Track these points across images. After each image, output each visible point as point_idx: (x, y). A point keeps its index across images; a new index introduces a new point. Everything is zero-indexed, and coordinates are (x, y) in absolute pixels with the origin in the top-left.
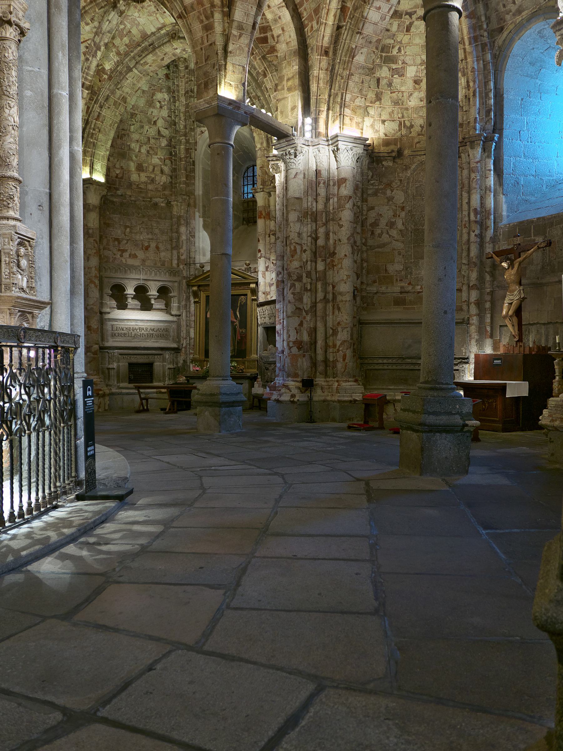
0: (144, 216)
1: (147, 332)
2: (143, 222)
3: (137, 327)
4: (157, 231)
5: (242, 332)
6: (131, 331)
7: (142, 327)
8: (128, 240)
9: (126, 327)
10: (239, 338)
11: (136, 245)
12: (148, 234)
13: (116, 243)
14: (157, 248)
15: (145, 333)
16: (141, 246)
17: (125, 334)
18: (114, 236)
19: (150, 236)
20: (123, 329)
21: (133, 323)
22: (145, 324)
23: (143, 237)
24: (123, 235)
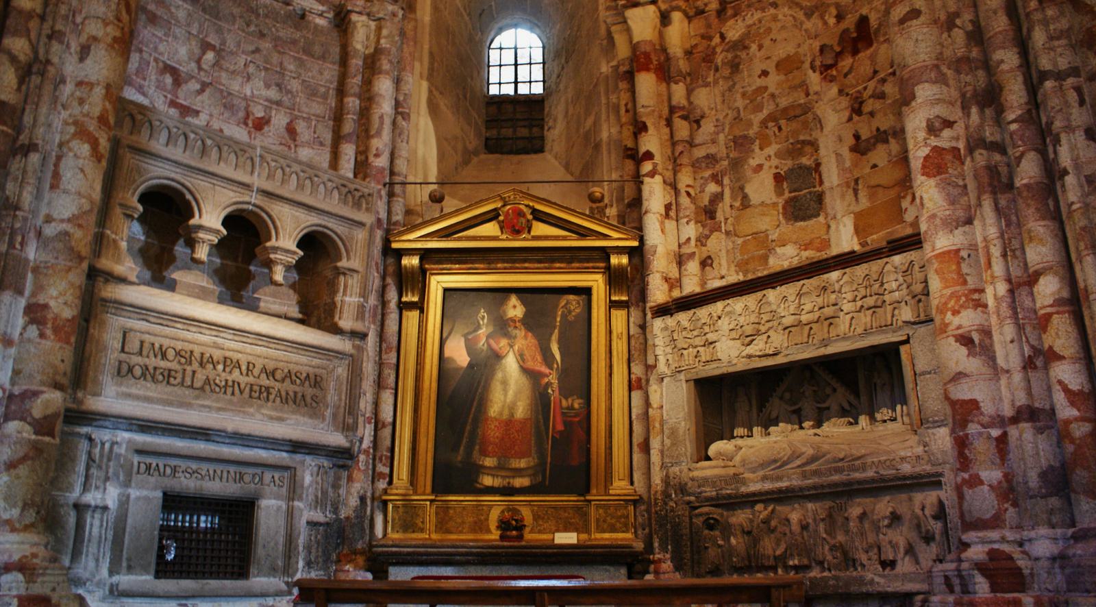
0: (262, 35)
1: (251, 379)
2: (257, 50)
3: (217, 354)
4: (295, 85)
5: (571, 408)
6: (195, 365)
7: (235, 356)
8: (204, 86)
9: (179, 346)
10: (560, 427)
11: (229, 107)
12: (268, 86)
13: (168, 80)
14: (291, 130)
15: (243, 380)
16: (241, 114)
17: (168, 375)
18: (165, 58)
19: (273, 93)
20: (164, 356)
21: (206, 338)
22: (249, 348)
23: (257, 89)
24: (193, 65)
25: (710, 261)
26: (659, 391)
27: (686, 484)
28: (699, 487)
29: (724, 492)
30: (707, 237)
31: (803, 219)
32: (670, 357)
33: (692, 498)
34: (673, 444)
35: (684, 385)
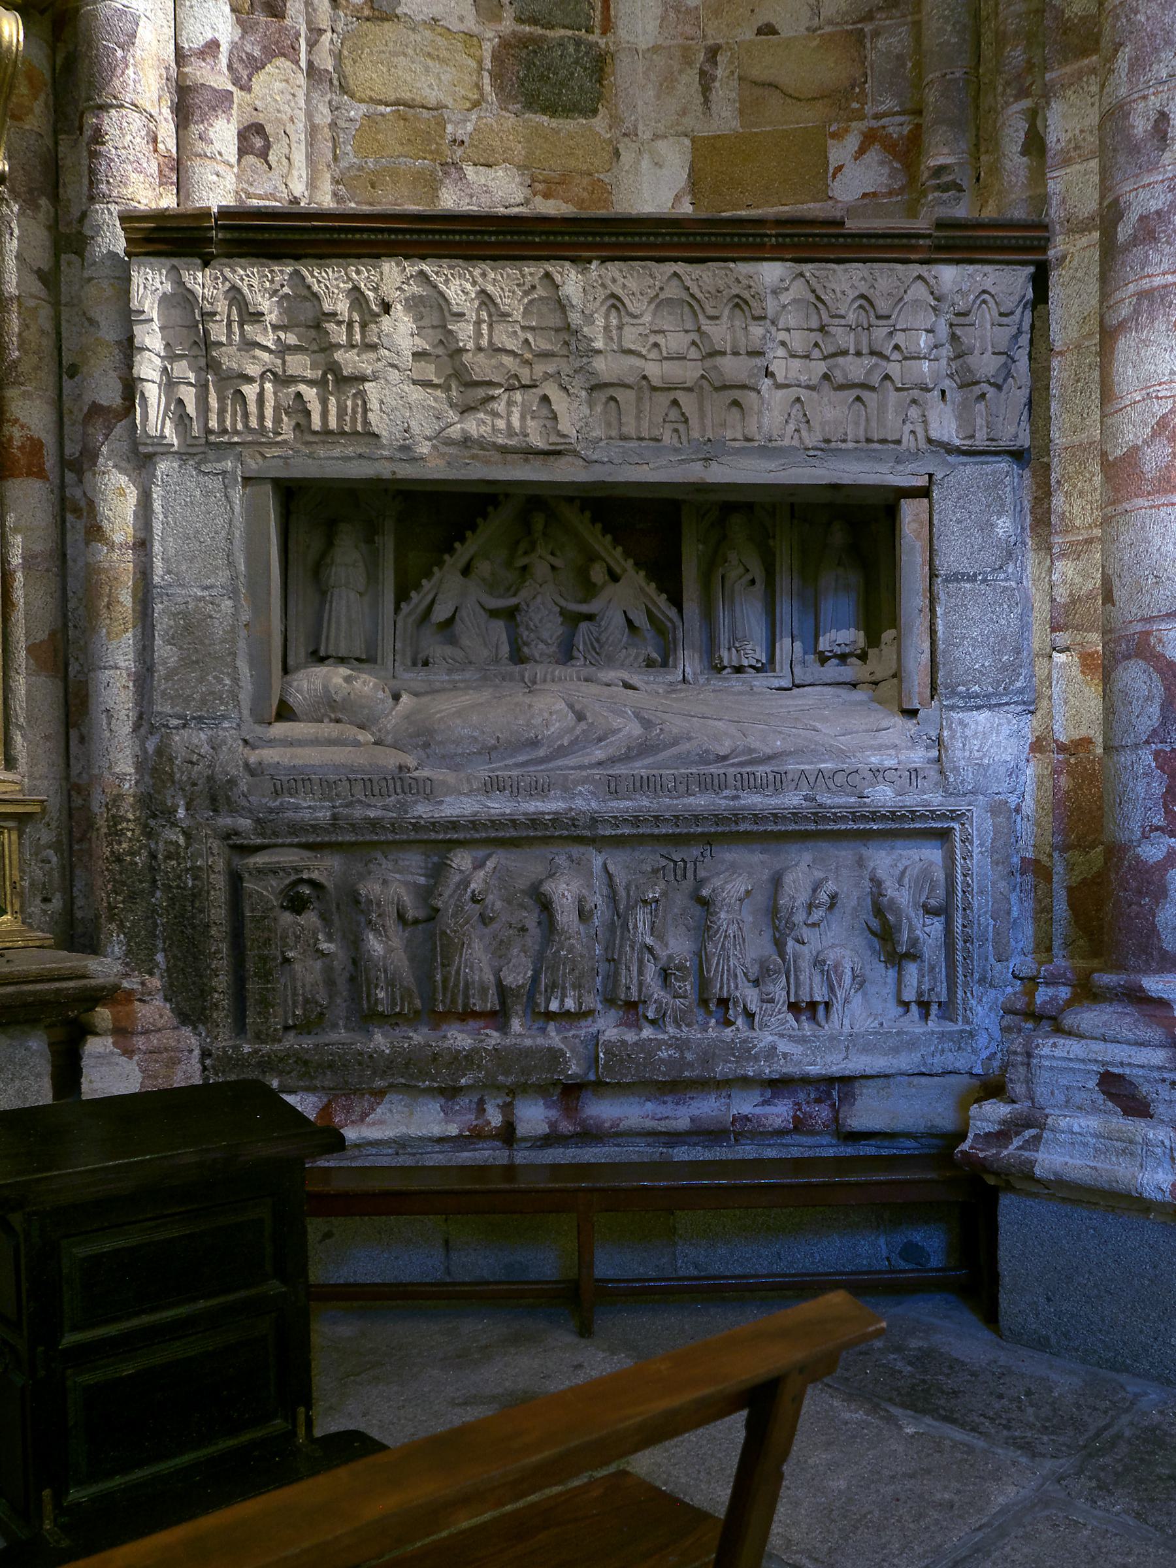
25: (258, 143)
26: (132, 495)
27: (232, 782)
28: (277, 793)
29: (358, 812)
30: (256, 66)
31: (551, 109)
32: (188, 395)
33: (245, 823)
34: (187, 662)
35: (237, 493)
